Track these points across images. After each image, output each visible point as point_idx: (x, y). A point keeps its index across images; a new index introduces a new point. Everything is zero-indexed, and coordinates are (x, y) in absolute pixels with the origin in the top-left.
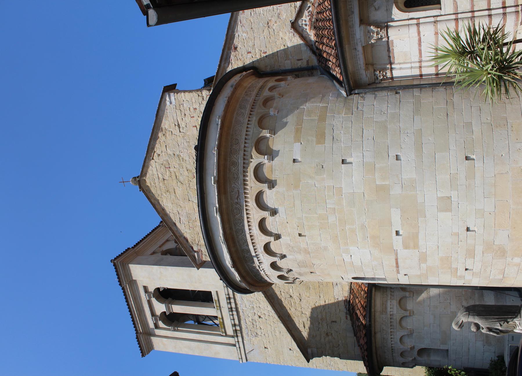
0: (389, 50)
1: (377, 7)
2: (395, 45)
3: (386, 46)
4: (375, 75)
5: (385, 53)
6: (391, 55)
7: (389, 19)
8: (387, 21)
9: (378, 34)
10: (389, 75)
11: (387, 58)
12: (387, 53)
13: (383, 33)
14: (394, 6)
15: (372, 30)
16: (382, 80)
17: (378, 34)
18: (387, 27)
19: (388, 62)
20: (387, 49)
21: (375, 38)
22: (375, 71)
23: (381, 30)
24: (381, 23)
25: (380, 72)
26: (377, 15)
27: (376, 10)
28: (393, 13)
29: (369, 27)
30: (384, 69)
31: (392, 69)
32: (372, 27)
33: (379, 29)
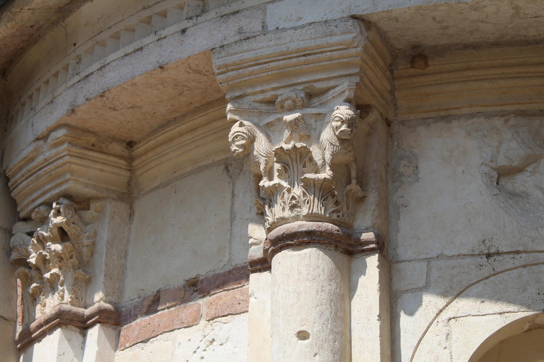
0: (197, 288)
1: (521, 182)
2: (222, 328)
3: (220, 266)
4: (48, 205)
5: (177, 268)
6: (163, 315)
7: (411, 273)
8: (405, 246)
9: (294, 161)
10: (49, 305)
11: (151, 285)
12: (179, 281)
13: (295, 208)
14: (516, 313)
15: (322, 118)
16: (23, 262)
17: (294, 161)
18: (345, 247)
19: (133, 291)
20: (203, 270)
21: (262, 146)
22: (78, 203)
23: (323, 191)
24: (388, 213)
25: (62, 235)
26: (450, 180)
27: (503, 174)
28: (463, 305)
29: (345, 87)
30: (82, 276)
31: (76, 324)
32: (344, 111)
33: (326, 174)
